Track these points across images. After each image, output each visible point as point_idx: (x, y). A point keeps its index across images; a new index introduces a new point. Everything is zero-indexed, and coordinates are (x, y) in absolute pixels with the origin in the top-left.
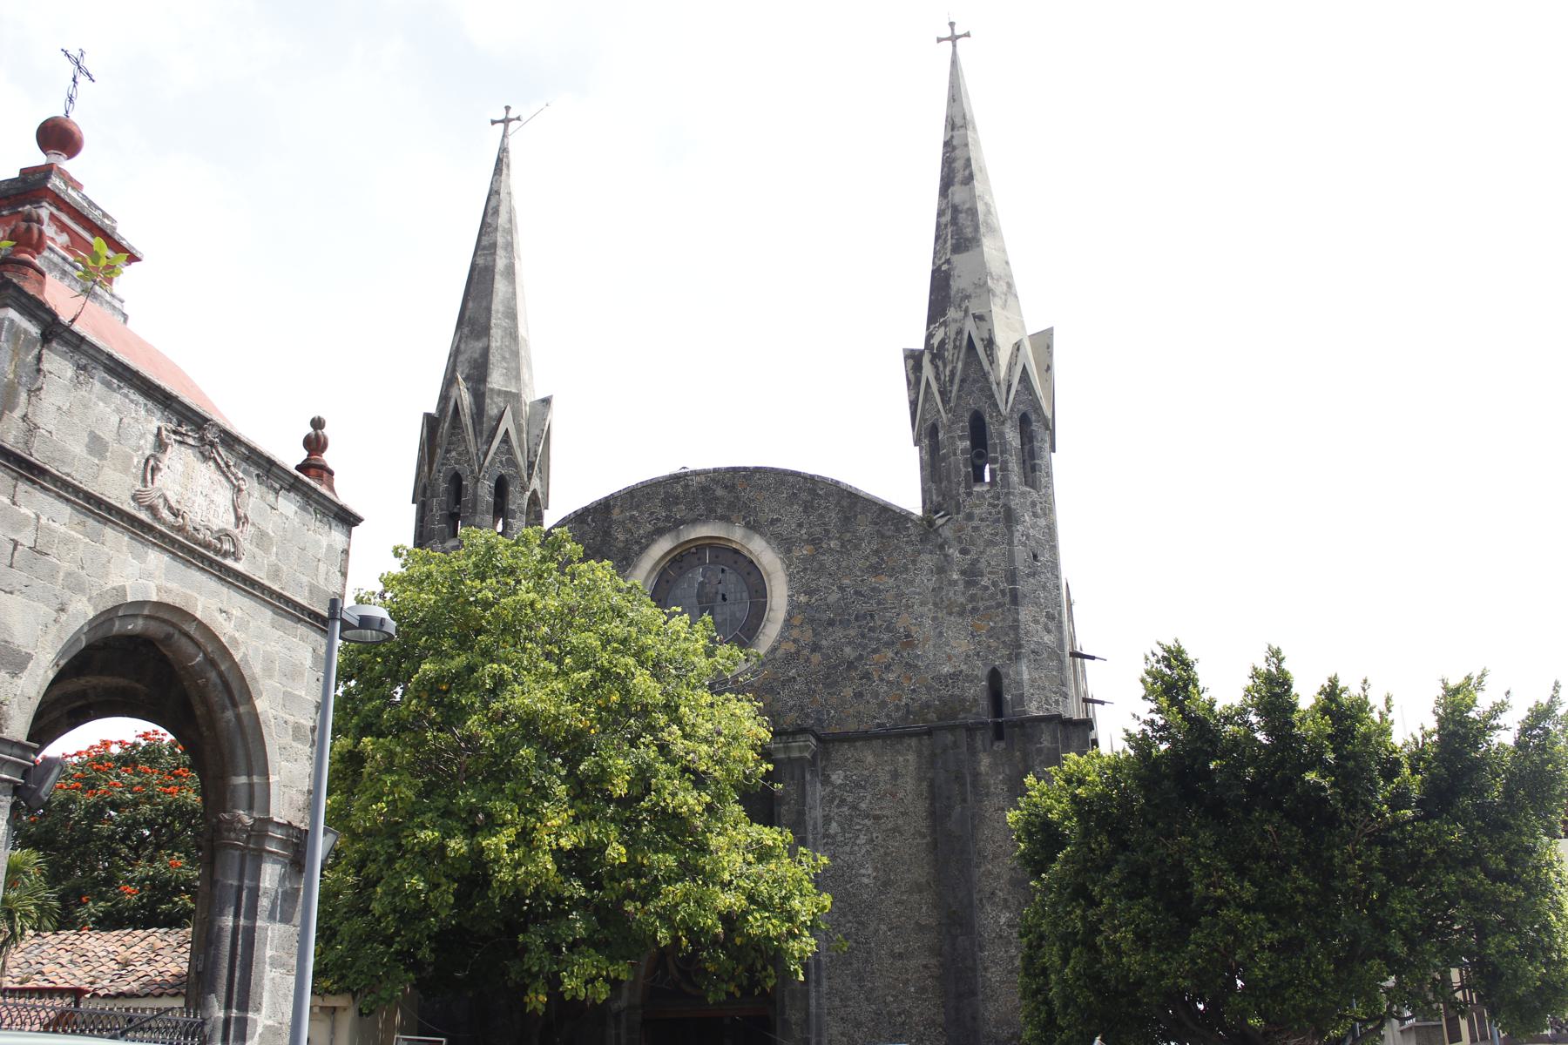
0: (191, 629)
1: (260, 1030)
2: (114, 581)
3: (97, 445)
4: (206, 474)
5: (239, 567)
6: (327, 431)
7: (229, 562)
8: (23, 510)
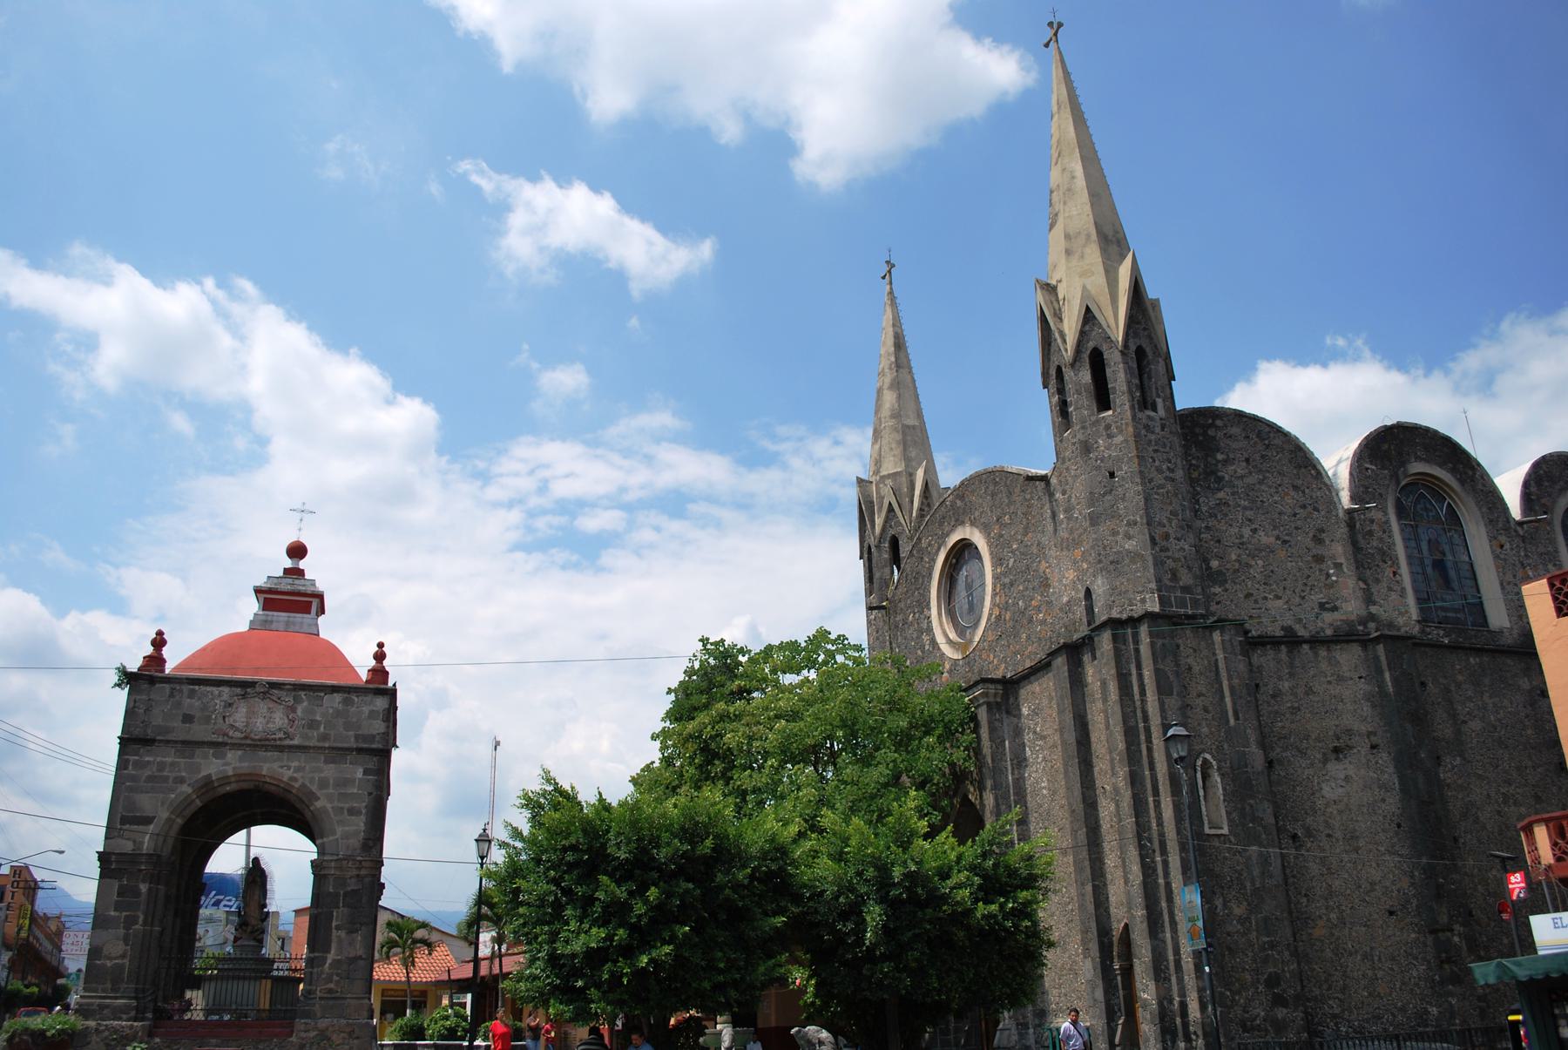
2: (204, 773)
3: (188, 719)
5: (296, 742)
7: (287, 742)
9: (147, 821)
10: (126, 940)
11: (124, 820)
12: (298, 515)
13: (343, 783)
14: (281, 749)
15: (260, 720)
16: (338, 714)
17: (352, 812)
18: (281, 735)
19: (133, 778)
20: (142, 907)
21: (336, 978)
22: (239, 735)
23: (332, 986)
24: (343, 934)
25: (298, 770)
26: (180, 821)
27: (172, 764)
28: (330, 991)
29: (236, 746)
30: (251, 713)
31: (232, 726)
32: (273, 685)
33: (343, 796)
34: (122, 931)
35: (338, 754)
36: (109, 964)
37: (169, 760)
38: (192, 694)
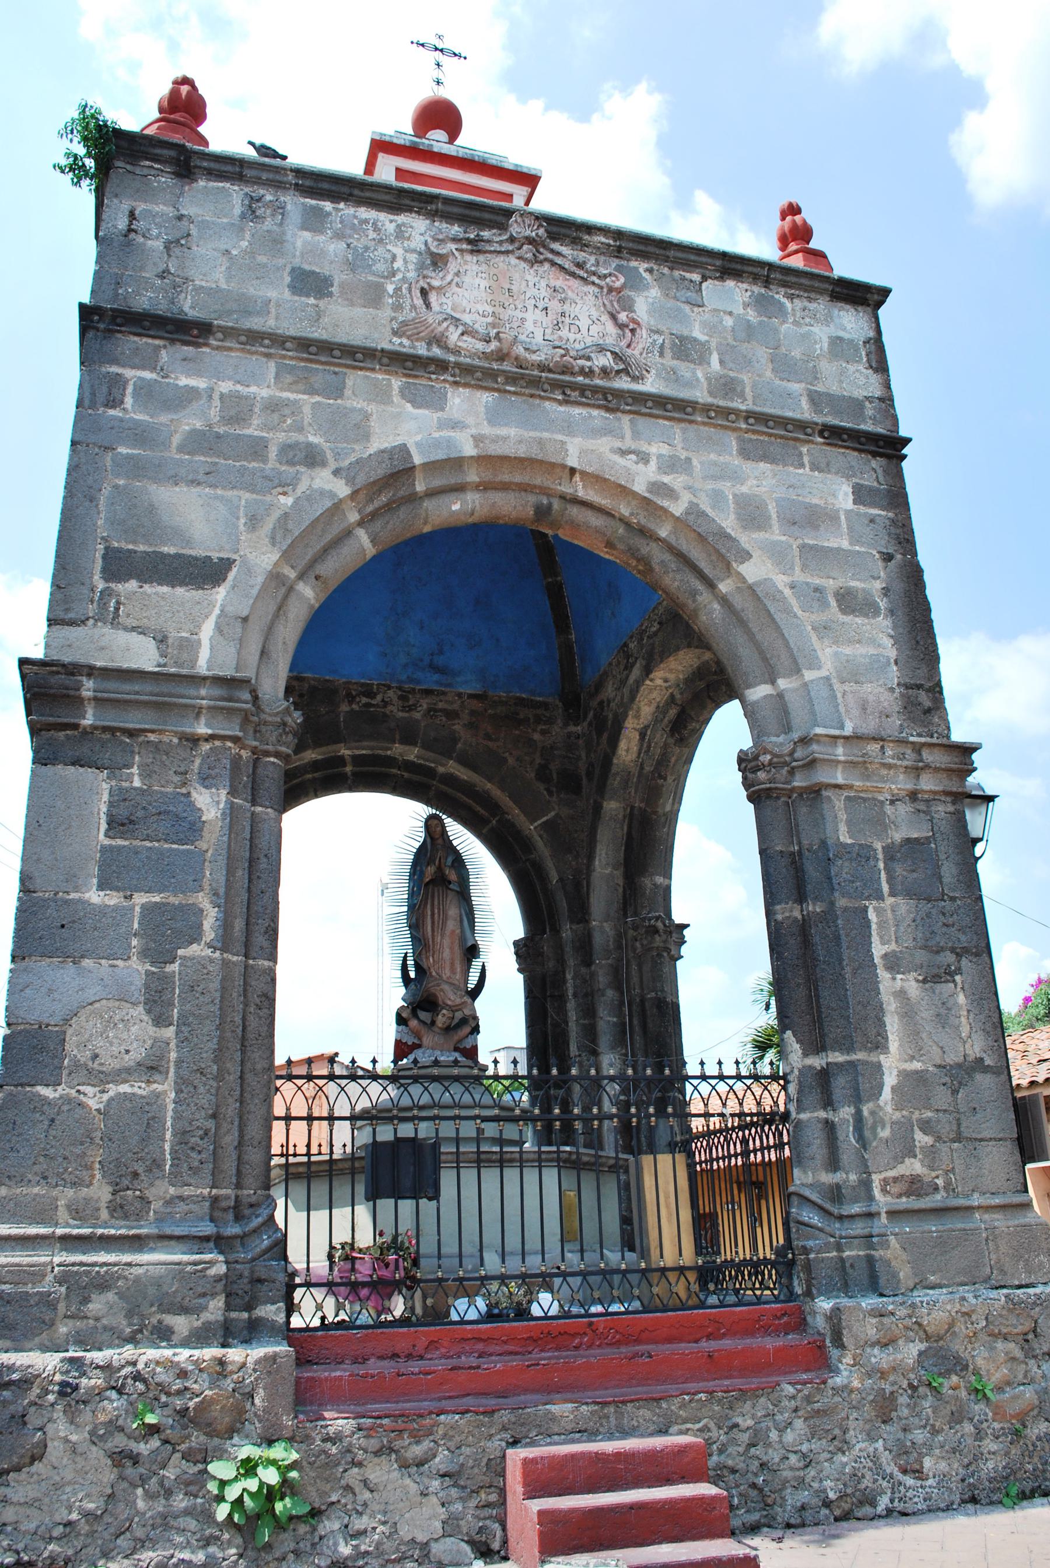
0: (580, 490)
1: (890, 1080)
2: (380, 442)
3: (310, 283)
6: (808, 215)
7: (623, 383)
8: (183, 381)
9: (208, 572)
10: (157, 1000)
11: (119, 565)
13: (814, 518)
14: (612, 401)
15: (533, 316)
18: (604, 360)
20: (213, 874)
21: (922, 1139)
23: (914, 1166)
24: (911, 984)
25: (671, 465)
26: (308, 593)
27: (273, 406)
28: (914, 1186)
30: (503, 293)
33: (813, 555)
35: (772, 432)
36: (93, 1099)
37: (262, 392)
38: (314, 221)
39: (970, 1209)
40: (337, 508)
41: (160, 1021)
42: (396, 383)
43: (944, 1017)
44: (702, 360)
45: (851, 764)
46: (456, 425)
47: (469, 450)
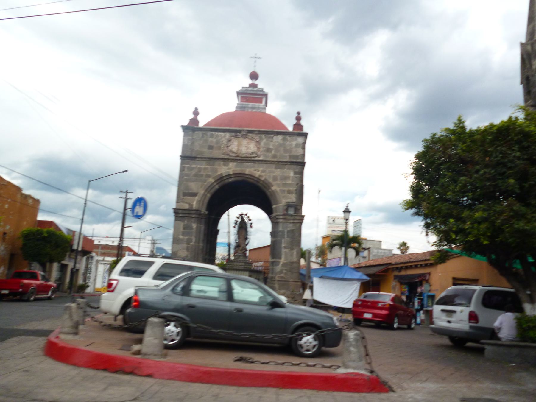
1: (281, 263)
2: (219, 173)
3: (211, 147)
4: (245, 142)
5: (261, 158)
6: (301, 115)
7: (257, 159)
8: (193, 166)
9: (194, 195)
10: (187, 249)
11: (185, 194)
12: (254, 60)
14: (255, 162)
16: (280, 145)
17: (289, 192)
18: (254, 155)
19: (187, 175)
20: (194, 234)
21: (284, 271)
22: (233, 155)
23: (282, 275)
25: (263, 171)
26: (209, 195)
27: (205, 169)
28: (282, 277)
29: (233, 160)
30: (239, 145)
31: (231, 151)
32: (250, 132)
33: (285, 185)
34: (185, 246)
35: (281, 164)
37: (203, 166)
38: (212, 136)
39: (289, 281)
40: (213, 183)
41: (188, 251)
42: (222, 163)
43: (292, 255)
44: (271, 152)
45: (283, 219)
46: (230, 169)
47: (231, 173)
